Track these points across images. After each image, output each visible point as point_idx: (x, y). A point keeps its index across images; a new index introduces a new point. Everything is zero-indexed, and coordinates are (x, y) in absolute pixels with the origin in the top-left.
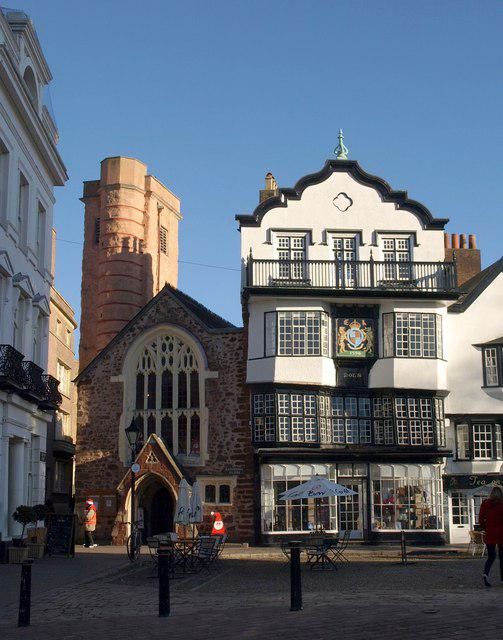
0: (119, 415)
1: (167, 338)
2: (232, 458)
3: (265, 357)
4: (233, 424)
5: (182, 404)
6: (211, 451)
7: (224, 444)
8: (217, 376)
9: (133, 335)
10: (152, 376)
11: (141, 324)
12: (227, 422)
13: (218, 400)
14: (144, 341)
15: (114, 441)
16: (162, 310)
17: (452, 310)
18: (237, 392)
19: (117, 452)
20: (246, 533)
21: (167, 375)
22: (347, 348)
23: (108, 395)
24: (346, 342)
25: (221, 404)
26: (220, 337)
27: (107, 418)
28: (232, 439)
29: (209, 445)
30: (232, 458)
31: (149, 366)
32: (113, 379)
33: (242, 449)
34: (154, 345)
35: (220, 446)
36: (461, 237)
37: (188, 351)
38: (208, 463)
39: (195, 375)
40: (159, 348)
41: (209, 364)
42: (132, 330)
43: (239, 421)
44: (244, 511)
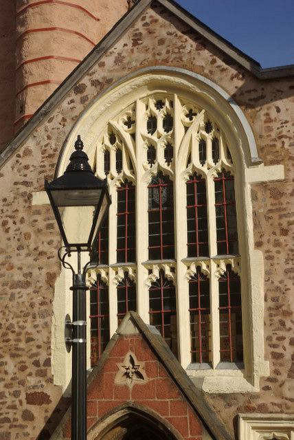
1: (159, 105)
6: (276, 356)
8: (282, 177)
9: (83, 100)
11: (99, 74)
15: (40, 338)
19: (48, 363)
21: (163, 183)
23: (27, 236)
27: (28, 284)
29: (268, 339)
31: (119, 167)
34: (130, 122)
37: (208, 128)
38: (270, 383)
39: (227, 182)
42: (79, 89)
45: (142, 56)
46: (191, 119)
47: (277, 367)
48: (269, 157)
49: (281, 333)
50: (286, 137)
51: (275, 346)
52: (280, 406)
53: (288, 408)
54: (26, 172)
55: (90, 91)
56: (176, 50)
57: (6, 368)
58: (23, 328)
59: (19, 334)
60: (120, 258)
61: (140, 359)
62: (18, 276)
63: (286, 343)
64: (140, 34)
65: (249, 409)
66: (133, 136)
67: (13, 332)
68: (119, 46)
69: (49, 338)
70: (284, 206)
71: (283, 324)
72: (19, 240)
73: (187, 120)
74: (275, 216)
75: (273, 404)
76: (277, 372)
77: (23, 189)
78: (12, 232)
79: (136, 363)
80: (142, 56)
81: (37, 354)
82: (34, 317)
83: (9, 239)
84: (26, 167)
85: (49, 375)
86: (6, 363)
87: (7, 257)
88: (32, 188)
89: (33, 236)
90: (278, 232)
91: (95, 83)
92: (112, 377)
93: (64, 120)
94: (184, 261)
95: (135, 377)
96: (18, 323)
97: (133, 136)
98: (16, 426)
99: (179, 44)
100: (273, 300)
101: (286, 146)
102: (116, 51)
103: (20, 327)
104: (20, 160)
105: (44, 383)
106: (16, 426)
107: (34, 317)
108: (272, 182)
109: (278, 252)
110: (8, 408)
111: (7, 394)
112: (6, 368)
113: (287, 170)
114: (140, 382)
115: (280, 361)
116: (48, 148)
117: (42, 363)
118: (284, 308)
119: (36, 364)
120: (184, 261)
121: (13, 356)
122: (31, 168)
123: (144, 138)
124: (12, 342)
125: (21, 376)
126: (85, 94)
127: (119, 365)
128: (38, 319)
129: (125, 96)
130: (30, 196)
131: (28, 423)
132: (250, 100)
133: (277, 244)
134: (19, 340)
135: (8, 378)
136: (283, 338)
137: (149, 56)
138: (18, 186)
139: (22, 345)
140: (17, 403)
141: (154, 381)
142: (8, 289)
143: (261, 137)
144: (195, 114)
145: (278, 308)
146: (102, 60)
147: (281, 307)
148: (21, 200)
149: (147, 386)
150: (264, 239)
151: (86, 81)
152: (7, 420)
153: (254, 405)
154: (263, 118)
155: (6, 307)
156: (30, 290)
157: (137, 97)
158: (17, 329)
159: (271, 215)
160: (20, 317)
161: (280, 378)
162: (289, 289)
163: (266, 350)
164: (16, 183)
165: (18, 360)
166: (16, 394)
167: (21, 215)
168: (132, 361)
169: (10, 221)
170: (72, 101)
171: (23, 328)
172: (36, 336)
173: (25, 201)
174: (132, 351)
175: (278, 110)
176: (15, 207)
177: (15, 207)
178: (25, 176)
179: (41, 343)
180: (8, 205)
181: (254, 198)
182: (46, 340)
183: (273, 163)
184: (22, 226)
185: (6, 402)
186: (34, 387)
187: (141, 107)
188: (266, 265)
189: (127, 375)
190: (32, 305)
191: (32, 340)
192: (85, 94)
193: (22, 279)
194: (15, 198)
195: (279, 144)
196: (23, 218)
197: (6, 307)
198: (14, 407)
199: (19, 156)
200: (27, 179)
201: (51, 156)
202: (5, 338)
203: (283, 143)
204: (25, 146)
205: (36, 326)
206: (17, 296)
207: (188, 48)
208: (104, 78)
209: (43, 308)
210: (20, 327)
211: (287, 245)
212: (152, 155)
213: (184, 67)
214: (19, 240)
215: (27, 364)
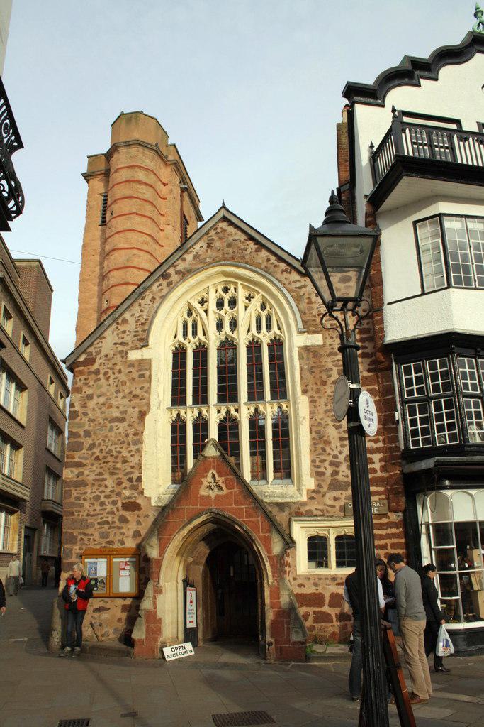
0: (142, 415)
3: (424, 293)
5: (255, 393)
6: (319, 475)
9: (169, 284)
10: (201, 352)
11: (181, 266)
13: (324, 383)
14: (187, 291)
15: (134, 461)
16: (218, 244)
19: (139, 479)
21: (228, 347)
23: (124, 383)
27: (122, 420)
29: (313, 461)
31: (195, 333)
32: (134, 355)
34: (203, 302)
37: (263, 307)
38: (315, 494)
39: (276, 345)
40: (212, 305)
41: (304, 323)
42: (165, 276)
45: (215, 254)
46: (250, 301)
47: (321, 483)
48: (311, 328)
51: (318, 467)
52: (322, 511)
53: (328, 512)
54: (125, 335)
55: (174, 277)
56: (240, 251)
57: (106, 483)
58: (120, 452)
59: (117, 457)
60: (195, 402)
61: (220, 476)
62: (116, 413)
63: (327, 464)
64: (213, 239)
65: (298, 514)
66: (206, 312)
67: (112, 456)
68: (197, 247)
70: (323, 364)
71: (324, 450)
72: (117, 386)
73: (247, 301)
74: (317, 371)
76: (320, 486)
77: (120, 348)
78: (111, 380)
79: (217, 478)
80: (215, 254)
81: (131, 473)
82: (129, 444)
83: (109, 385)
84: (124, 332)
85: (140, 489)
86: (106, 479)
87: (107, 399)
88: (128, 347)
89: (128, 384)
90: (319, 383)
91: (178, 273)
92: (197, 490)
93: (153, 298)
94: (245, 403)
95: (216, 489)
97: (206, 312)
98: (114, 527)
99: (243, 247)
100: (316, 432)
102: (195, 251)
103: (117, 452)
104: (119, 327)
105: (136, 495)
106: (114, 527)
107: (129, 444)
108: (314, 346)
109: (320, 397)
110: (108, 513)
111: (107, 503)
112: (106, 483)
113: (325, 338)
114: (221, 493)
115: (322, 478)
116: (141, 318)
117: (134, 480)
118: (325, 438)
119: (130, 480)
120: (245, 403)
122: (128, 333)
123: (215, 313)
124: (111, 464)
125: (117, 489)
126: (170, 280)
127: (203, 480)
128: (132, 446)
129: (200, 282)
130: (127, 353)
131: (123, 525)
132: (296, 288)
133: (318, 391)
134: (117, 462)
135: (108, 491)
136: (324, 461)
137: (220, 254)
139: (119, 465)
140: (115, 510)
141: (231, 492)
142: (108, 423)
143: (305, 314)
144: (253, 298)
145: (320, 438)
146: (184, 256)
147: (322, 438)
148: (119, 356)
149: (226, 496)
150: (309, 388)
151: (171, 271)
152: (107, 522)
153: (303, 510)
154: (306, 301)
155: (106, 436)
156: (125, 424)
157: (209, 284)
158: (115, 454)
159: (313, 370)
160: (116, 444)
161: (322, 490)
162: (328, 425)
163: (311, 470)
164: (115, 344)
165: (115, 477)
166: (114, 503)
167: (118, 367)
168: (214, 477)
169: (110, 372)
170: (160, 285)
171: (120, 452)
172: (130, 459)
173: (122, 357)
174: (214, 469)
176: (114, 361)
177: (114, 361)
178: (123, 338)
179: (134, 465)
181: (301, 358)
182: (138, 462)
183: (314, 332)
184: (119, 375)
185: (105, 509)
186: (129, 498)
187: (212, 291)
188: (310, 406)
189: (210, 487)
190: (127, 435)
191: (127, 462)
192: (170, 280)
193: (118, 415)
194: (114, 355)
196: (120, 370)
197: (106, 436)
198: (112, 513)
199: (118, 324)
200: (123, 341)
201: (143, 324)
202: (106, 460)
205: (130, 452)
206: (115, 428)
207: (249, 251)
208: (184, 269)
209: (135, 438)
210: (117, 452)
211: (326, 392)
212: (220, 326)
213: (247, 263)
214: (117, 386)
215: (122, 480)
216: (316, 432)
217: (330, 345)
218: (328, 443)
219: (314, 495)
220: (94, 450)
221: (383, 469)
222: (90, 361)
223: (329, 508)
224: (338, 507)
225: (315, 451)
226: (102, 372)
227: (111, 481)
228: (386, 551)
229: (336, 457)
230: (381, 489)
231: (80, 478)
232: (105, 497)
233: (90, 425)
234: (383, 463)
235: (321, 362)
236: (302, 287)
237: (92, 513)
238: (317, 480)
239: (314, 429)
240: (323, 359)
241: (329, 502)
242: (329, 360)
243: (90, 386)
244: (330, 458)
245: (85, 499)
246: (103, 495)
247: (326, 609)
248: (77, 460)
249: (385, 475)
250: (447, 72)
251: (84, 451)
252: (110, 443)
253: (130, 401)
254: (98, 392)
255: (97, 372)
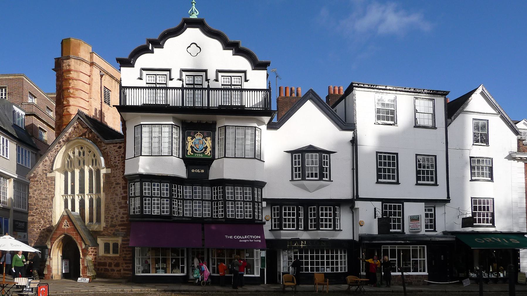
0: (52, 198)
1: (82, 148)
2: (120, 225)
4: (120, 203)
6: (106, 221)
7: (115, 216)
12: (116, 202)
13: (110, 188)
15: (50, 214)
17: (272, 126)
18: (122, 182)
20: (128, 274)
22: (192, 151)
24: (191, 147)
25: (112, 190)
26: (112, 146)
27: (46, 199)
28: (119, 213)
29: (105, 217)
30: (120, 225)
32: (49, 175)
33: (125, 219)
35: (112, 218)
36: (291, 89)
38: (106, 228)
43: (123, 201)
44: (126, 260)
49: (108, 215)
50: (112, 161)
52: (107, 234)
53: (109, 235)
58: (45, 211)
62: (44, 197)
69: (52, 215)
75: (106, 234)
76: (107, 226)
77: (45, 172)
81: (49, 219)
83: (41, 186)
84: (46, 165)
86: (41, 221)
89: (47, 185)
93: (56, 152)
96: (44, 210)
98: (44, 238)
101: (112, 163)
102: (69, 132)
106: (44, 238)
113: (111, 170)
118: (109, 209)
119: (49, 221)
121: (43, 219)
122: (47, 166)
135: (42, 225)
136: (109, 217)
138: (43, 171)
139: (45, 216)
156: (47, 201)
160: (45, 208)
169: (42, 181)
170: (57, 146)
171: (45, 211)
172: (49, 214)
175: (110, 153)
179: (49, 216)
180: (41, 176)
184: (44, 183)
193: (45, 198)
195: (110, 163)
199: (44, 162)
200: (46, 169)
203: (111, 162)
204: (45, 159)
205: (48, 211)
209: (50, 206)
216: (108, 206)
217: (113, 173)
218: (110, 210)
219: (105, 229)
220: (37, 210)
221: (127, 220)
222: (35, 177)
223: (109, 233)
224: (112, 233)
225: (106, 213)
226: (39, 181)
227: (43, 221)
228: (126, 249)
229: (112, 215)
230: (126, 228)
231: (33, 221)
232: (41, 227)
233: (36, 201)
234: (127, 219)
235: (110, 180)
236: (105, 149)
237: (37, 233)
238: (107, 224)
239: (107, 205)
240: (111, 178)
241: (109, 231)
242: (113, 179)
243: (35, 186)
244: (111, 216)
245: (35, 228)
246: (40, 227)
247: (107, 267)
248: (32, 214)
249: (127, 223)
250: (170, 42)
251: (34, 211)
252: (42, 208)
253: (48, 192)
254: (38, 188)
255: (37, 181)
